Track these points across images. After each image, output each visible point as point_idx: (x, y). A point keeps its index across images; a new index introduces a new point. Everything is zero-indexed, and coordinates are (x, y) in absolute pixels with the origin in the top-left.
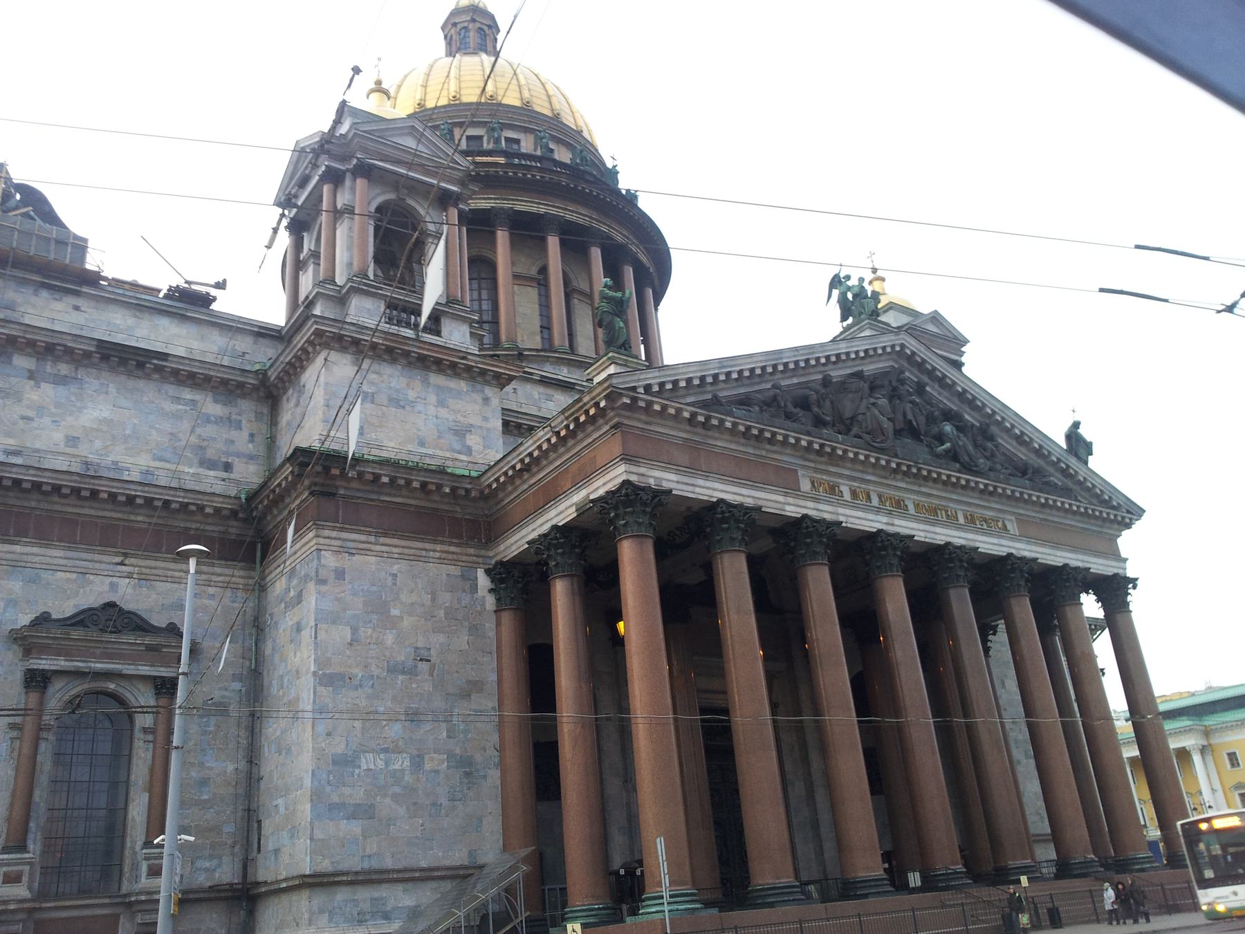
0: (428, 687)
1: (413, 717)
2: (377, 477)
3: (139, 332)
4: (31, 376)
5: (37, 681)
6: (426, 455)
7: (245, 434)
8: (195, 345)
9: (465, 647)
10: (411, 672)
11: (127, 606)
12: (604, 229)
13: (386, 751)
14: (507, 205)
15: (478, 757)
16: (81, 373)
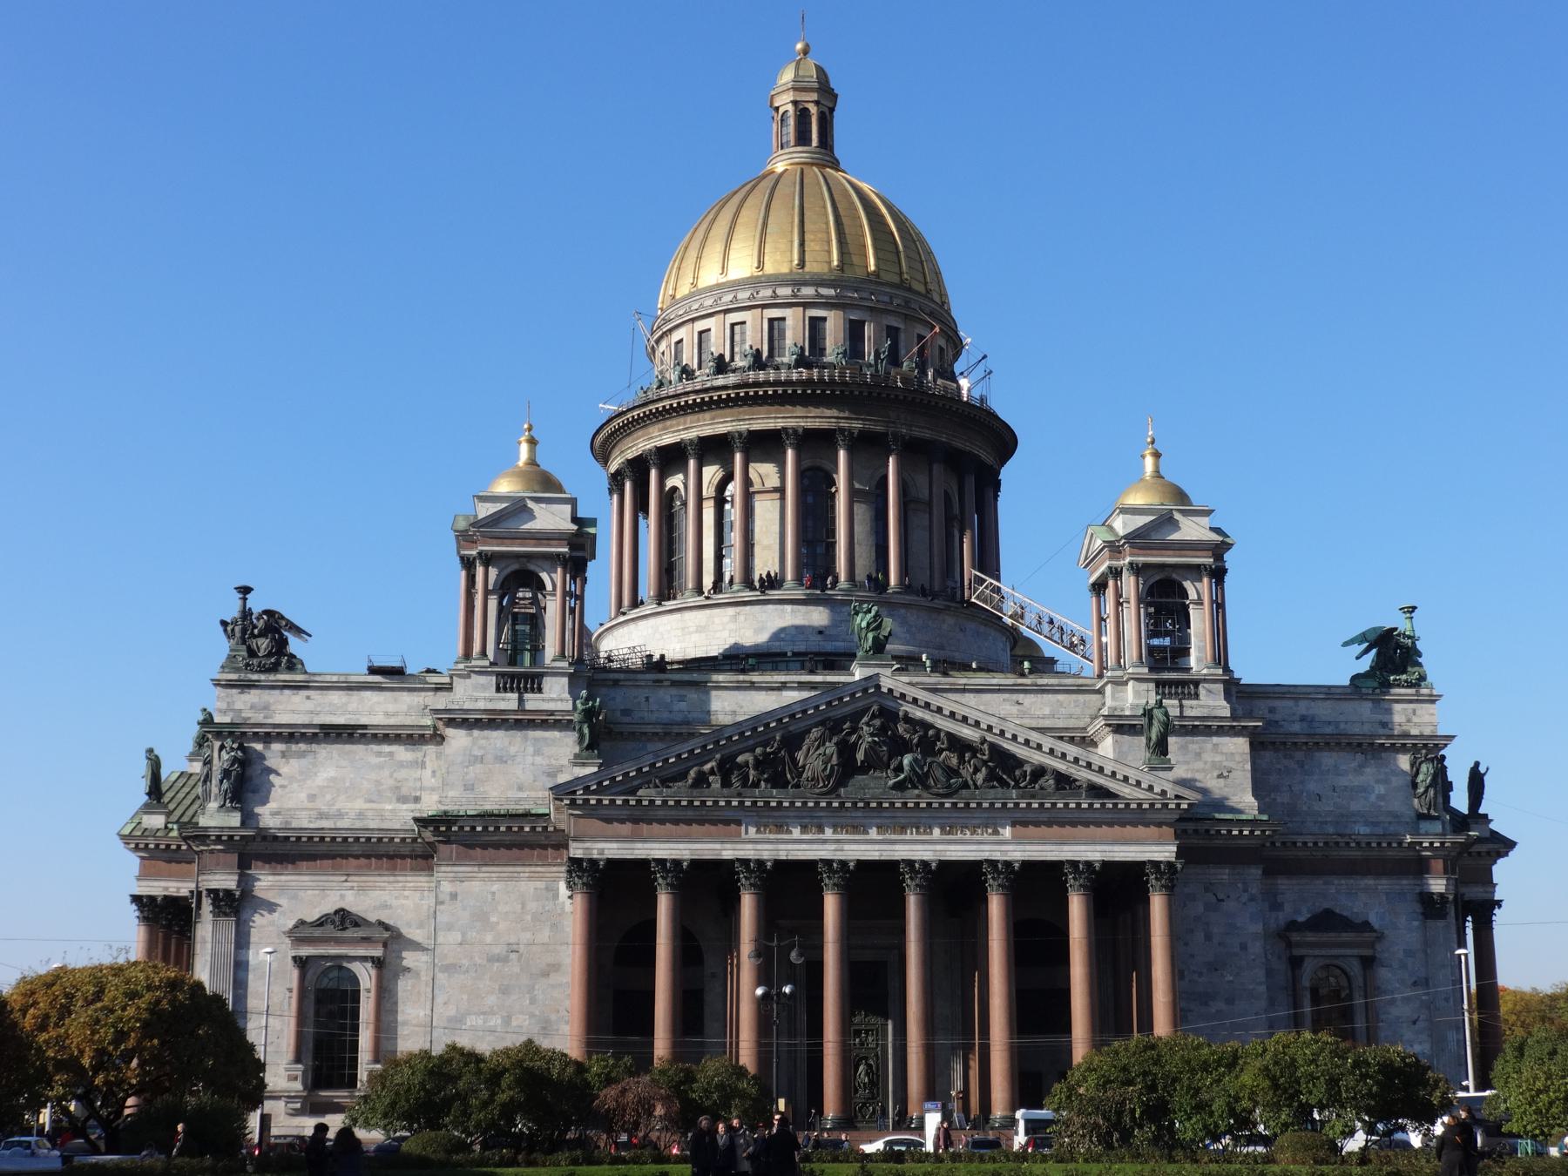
0: (517, 970)
1: (505, 991)
2: (473, 828)
3: (351, 707)
4: (284, 755)
5: (301, 963)
6: (520, 799)
7: (428, 773)
8: (391, 708)
9: (546, 940)
10: (504, 960)
11: (353, 909)
12: (857, 425)
13: (484, 1013)
14: (743, 427)
15: (553, 1017)
16: (314, 746)
